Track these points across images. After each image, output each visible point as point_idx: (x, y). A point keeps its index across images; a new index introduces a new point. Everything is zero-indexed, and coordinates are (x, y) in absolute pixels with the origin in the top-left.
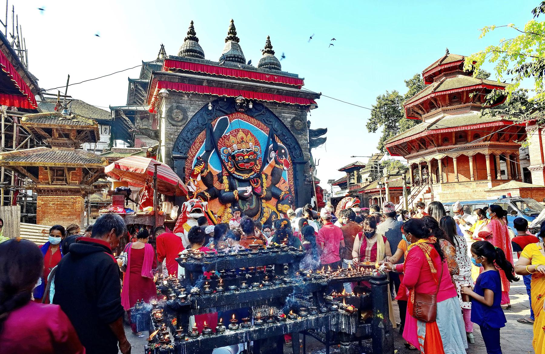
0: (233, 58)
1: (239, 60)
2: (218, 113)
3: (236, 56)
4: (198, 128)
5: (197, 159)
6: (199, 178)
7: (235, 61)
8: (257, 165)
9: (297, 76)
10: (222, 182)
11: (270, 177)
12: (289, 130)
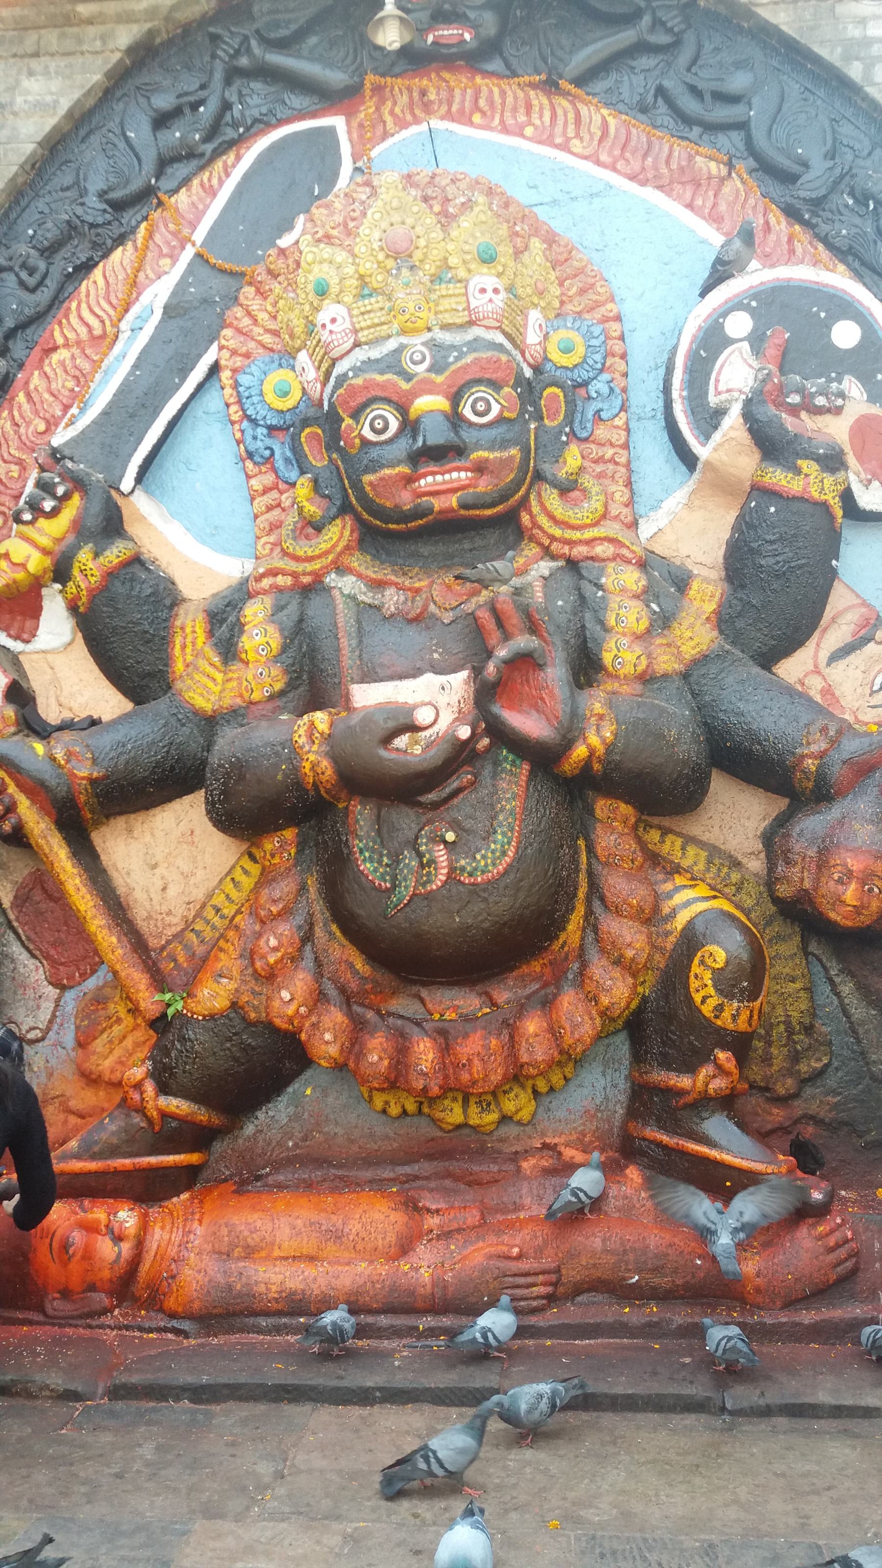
4: (72, 230)
11: (707, 593)
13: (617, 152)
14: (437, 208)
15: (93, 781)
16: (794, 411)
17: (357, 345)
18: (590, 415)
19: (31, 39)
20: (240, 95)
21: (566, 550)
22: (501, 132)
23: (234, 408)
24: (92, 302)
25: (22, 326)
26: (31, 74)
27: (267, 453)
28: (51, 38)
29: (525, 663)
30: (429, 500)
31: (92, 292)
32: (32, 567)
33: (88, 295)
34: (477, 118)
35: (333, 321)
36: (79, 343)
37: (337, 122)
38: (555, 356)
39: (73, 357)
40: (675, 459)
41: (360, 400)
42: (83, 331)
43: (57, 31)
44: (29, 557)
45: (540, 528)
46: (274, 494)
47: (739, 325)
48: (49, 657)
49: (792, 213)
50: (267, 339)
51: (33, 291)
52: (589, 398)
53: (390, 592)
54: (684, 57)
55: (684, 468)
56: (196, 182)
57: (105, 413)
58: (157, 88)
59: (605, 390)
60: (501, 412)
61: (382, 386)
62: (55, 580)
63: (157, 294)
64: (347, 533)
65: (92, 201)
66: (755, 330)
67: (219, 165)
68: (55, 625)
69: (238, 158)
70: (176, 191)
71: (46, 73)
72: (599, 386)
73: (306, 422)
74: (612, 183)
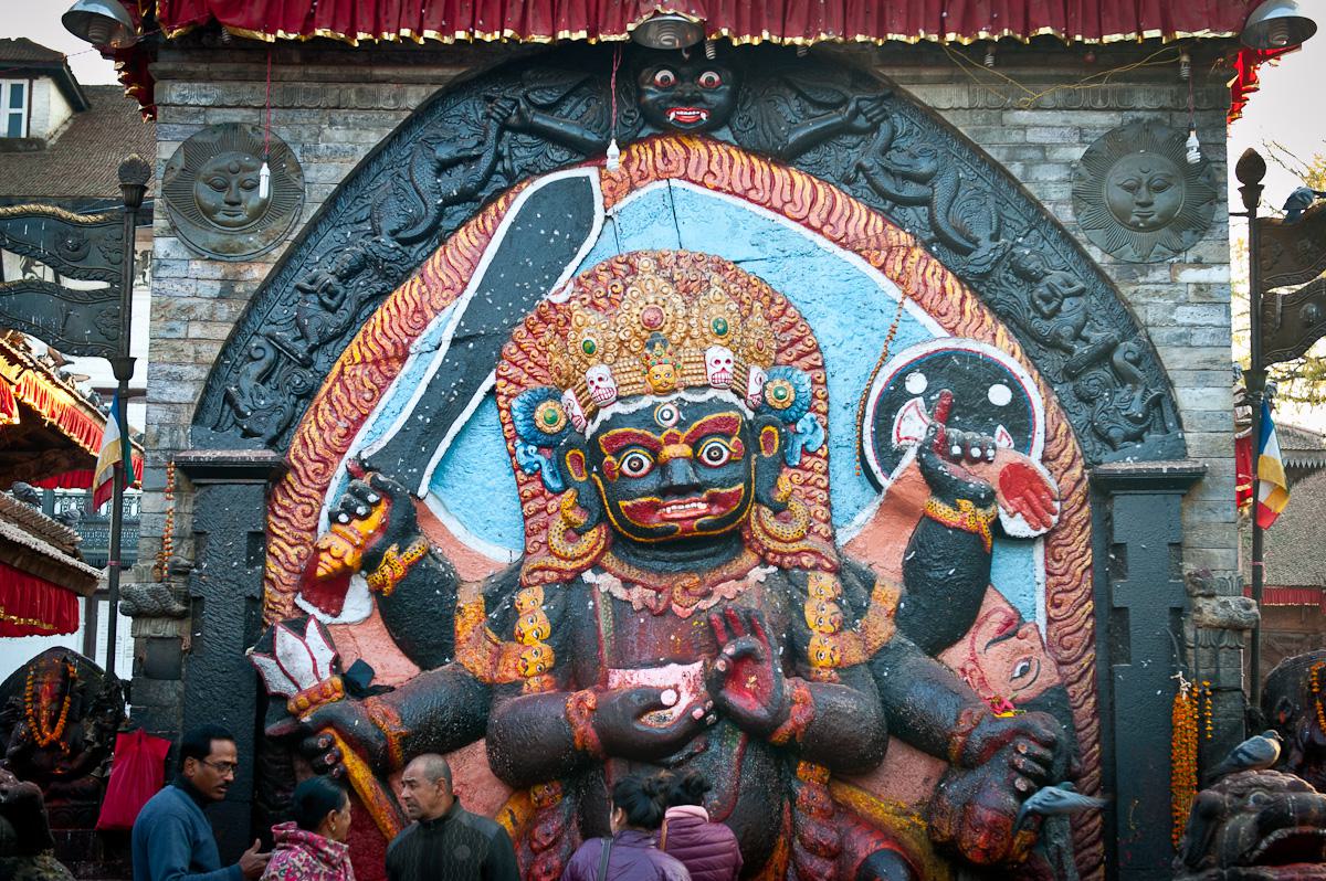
5: (351, 475)
10: (505, 626)
12: (1066, 237)
13: (824, 215)
14: (682, 288)
16: (956, 460)
17: (619, 398)
18: (798, 448)
19: (333, 93)
20: (510, 147)
21: (778, 559)
22: (728, 192)
23: (507, 427)
24: (386, 326)
25: (325, 341)
26: (332, 124)
27: (537, 466)
28: (351, 93)
29: (744, 657)
30: (663, 505)
31: (387, 319)
32: (348, 560)
33: (382, 320)
34: (709, 180)
35: (600, 379)
36: (376, 362)
37: (590, 172)
38: (770, 401)
39: (371, 374)
40: (867, 484)
41: (620, 444)
42: (376, 349)
43: (357, 86)
44: (345, 552)
45: (757, 540)
46: (541, 501)
47: (916, 383)
48: (351, 628)
49: (967, 281)
50: (538, 372)
51: (333, 311)
52: (797, 433)
53: (637, 592)
55: (872, 489)
56: (473, 223)
57: (403, 430)
58: (439, 140)
59: (810, 428)
60: (730, 456)
61: (640, 436)
62: (362, 568)
63: (446, 324)
64: (602, 542)
66: (928, 389)
67: (492, 209)
68: (358, 603)
69: (508, 204)
70: (456, 230)
71: (347, 125)
73: (570, 446)
74: (819, 245)
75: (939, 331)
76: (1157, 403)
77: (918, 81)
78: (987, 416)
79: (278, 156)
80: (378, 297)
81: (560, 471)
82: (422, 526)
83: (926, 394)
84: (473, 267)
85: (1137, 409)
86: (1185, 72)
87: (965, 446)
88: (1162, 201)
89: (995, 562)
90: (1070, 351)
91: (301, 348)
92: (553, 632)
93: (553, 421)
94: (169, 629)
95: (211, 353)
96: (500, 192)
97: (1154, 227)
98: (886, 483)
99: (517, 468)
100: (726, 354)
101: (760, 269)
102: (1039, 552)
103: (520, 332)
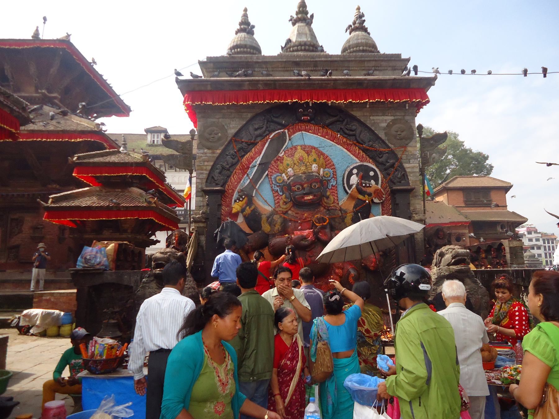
0: (298, 46)
1: (311, 48)
2: (272, 126)
3: (302, 43)
4: (241, 149)
5: (238, 192)
6: (240, 220)
7: (301, 50)
8: (328, 198)
9: (399, 56)
12: (383, 142)
15: (251, 246)
47: (355, 171)
51: (233, 159)
54: (345, 123)
65: (244, 144)
72: (332, 180)
75: (358, 161)
76: (404, 175)
77: (353, 111)
78: (369, 178)
79: (223, 129)
80: (243, 156)
81: (282, 191)
82: (254, 202)
83: (357, 174)
84: (262, 150)
85: (399, 176)
86: (407, 108)
87: (366, 184)
88: (403, 134)
89: (372, 208)
90: (385, 165)
91: (228, 166)
92: (282, 224)
93: (279, 180)
94: (201, 225)
95: (209, 168)
96: (267, 135)
97: (401, 139)
98: (349, 192)
99: (273, 190)
100: (316, 165)
101: (321, 149)
102: (380, 207)
103: (273, 162)
